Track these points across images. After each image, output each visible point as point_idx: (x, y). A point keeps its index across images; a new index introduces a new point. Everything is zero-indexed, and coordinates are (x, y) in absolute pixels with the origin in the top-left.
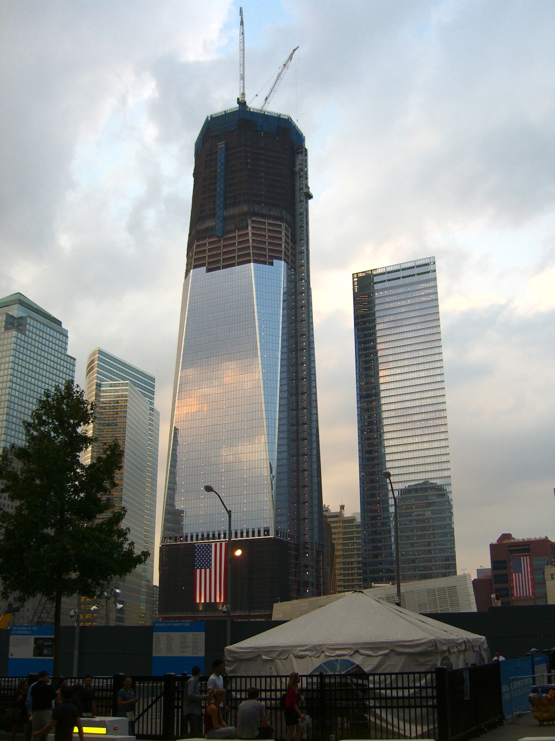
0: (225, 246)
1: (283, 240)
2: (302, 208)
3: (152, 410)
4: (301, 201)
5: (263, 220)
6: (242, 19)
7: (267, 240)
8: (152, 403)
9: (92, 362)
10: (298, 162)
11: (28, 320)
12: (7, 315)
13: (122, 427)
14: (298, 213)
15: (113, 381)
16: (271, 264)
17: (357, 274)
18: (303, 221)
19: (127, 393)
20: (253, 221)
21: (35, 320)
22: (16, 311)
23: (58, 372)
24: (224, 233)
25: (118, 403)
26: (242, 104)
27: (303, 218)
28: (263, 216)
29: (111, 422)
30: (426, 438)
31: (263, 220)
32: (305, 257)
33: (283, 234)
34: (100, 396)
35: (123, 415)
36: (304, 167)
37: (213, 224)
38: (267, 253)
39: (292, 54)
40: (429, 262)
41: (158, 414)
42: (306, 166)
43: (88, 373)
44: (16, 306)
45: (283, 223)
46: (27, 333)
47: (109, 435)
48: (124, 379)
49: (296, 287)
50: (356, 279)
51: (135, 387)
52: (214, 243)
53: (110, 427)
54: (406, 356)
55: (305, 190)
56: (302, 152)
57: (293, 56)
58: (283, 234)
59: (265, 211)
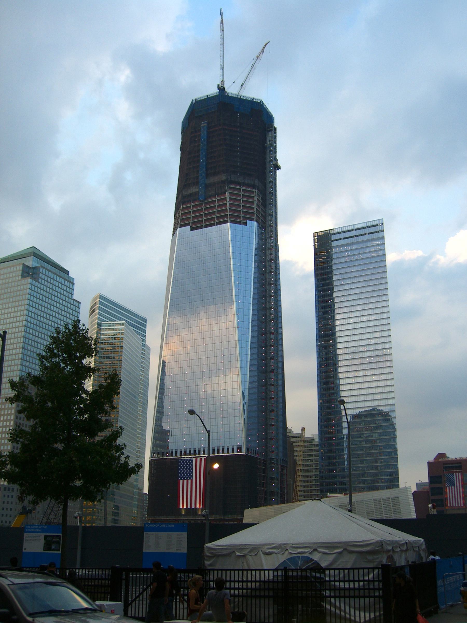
0: (206, 209)
1: (255, 204)
2: (271, 177)
3: (144, 345)
4: (271, 172)
5: (238, 187)
6: (222, 18)
7: (242, 204)
8: (144, 340)
9: (94, 305)
10: (268, 138)
11: (41, 269)
12: (24, 265)
13: (119, 360)
14: (268, 180)
15: (111, 321)
16: (245, 224)
17: (317, 233)
18: (272, 188)
19: (123, 331)
20: (230, 188)
21: (47, 269)
22: (31, 262)
23: (66, 313)
24: (206, 199)
25: (115, 339)
26: (222, 89)
27: (272, 186)
28: (239, 184)
29: (109, 355)
30: (374, 372)
31: (238, 187)
32: (274, 218)
33: (255, 199)
34: (100, 334)
35: (119, 350)
36: (273, 142)
37: (197, 190)
38: (242, 215)
39: (264, 48)
40: (378, 223)
41: (149, 349)
42: (275, 142)
43: (91, 314)
44: (32, 257)
45: (256, 190)
46: (40, 280)
47: (108, 367)
48: (120, 319)
49: (266, 244)
50: (316, 238)
52: (197, 206)
53: (109, 360)
54: (358, 302)
55: (274, 163)
56: (271, 130)
57: (265, 50)
58: (255, 199)
59: (240, 180)
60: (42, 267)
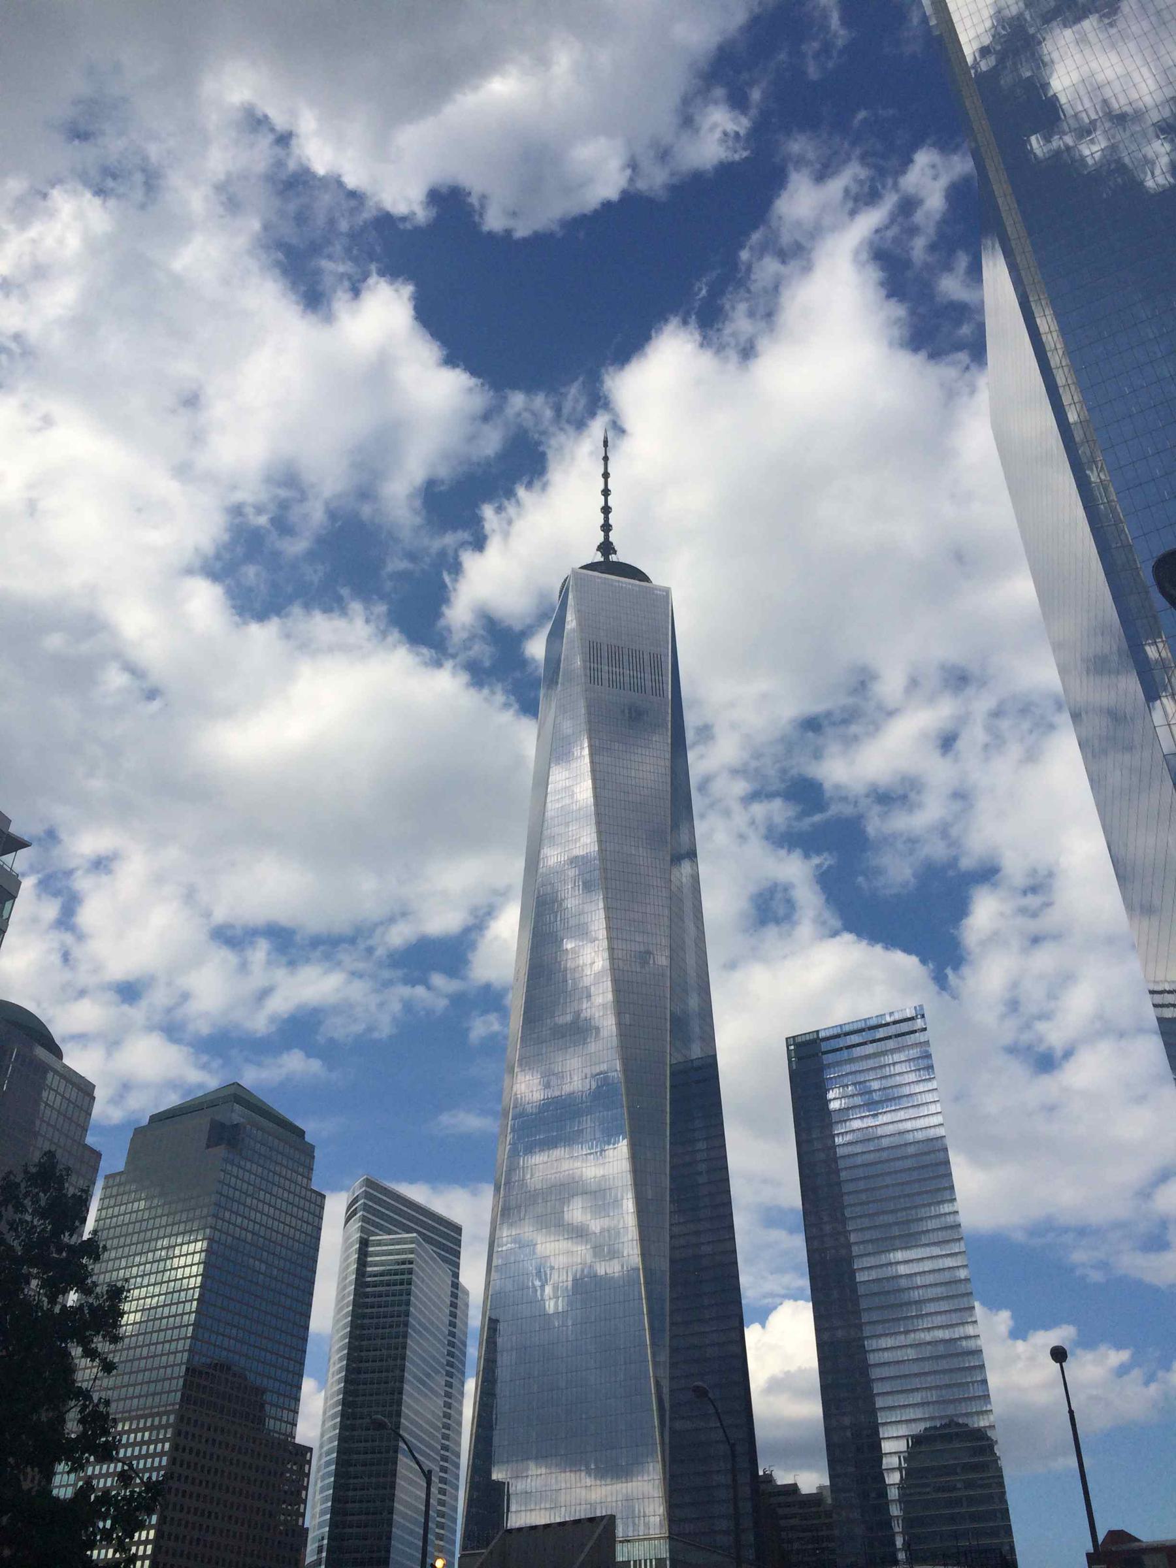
3: (456, 1285)
41: (467, 1293)
43: (347, 1221)
48: (409, 1230)
51: (426, 1245)
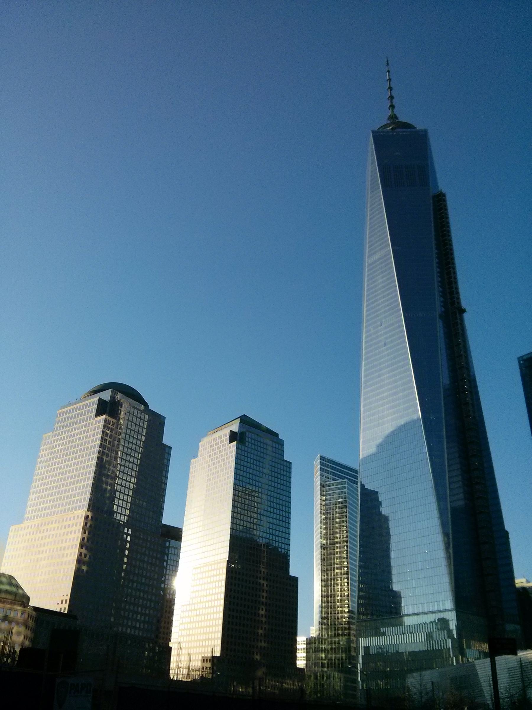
11: (247, 434)
17: (522, 357)
21: (253, 433)
46: (247, 444)
60: (247, 431)
